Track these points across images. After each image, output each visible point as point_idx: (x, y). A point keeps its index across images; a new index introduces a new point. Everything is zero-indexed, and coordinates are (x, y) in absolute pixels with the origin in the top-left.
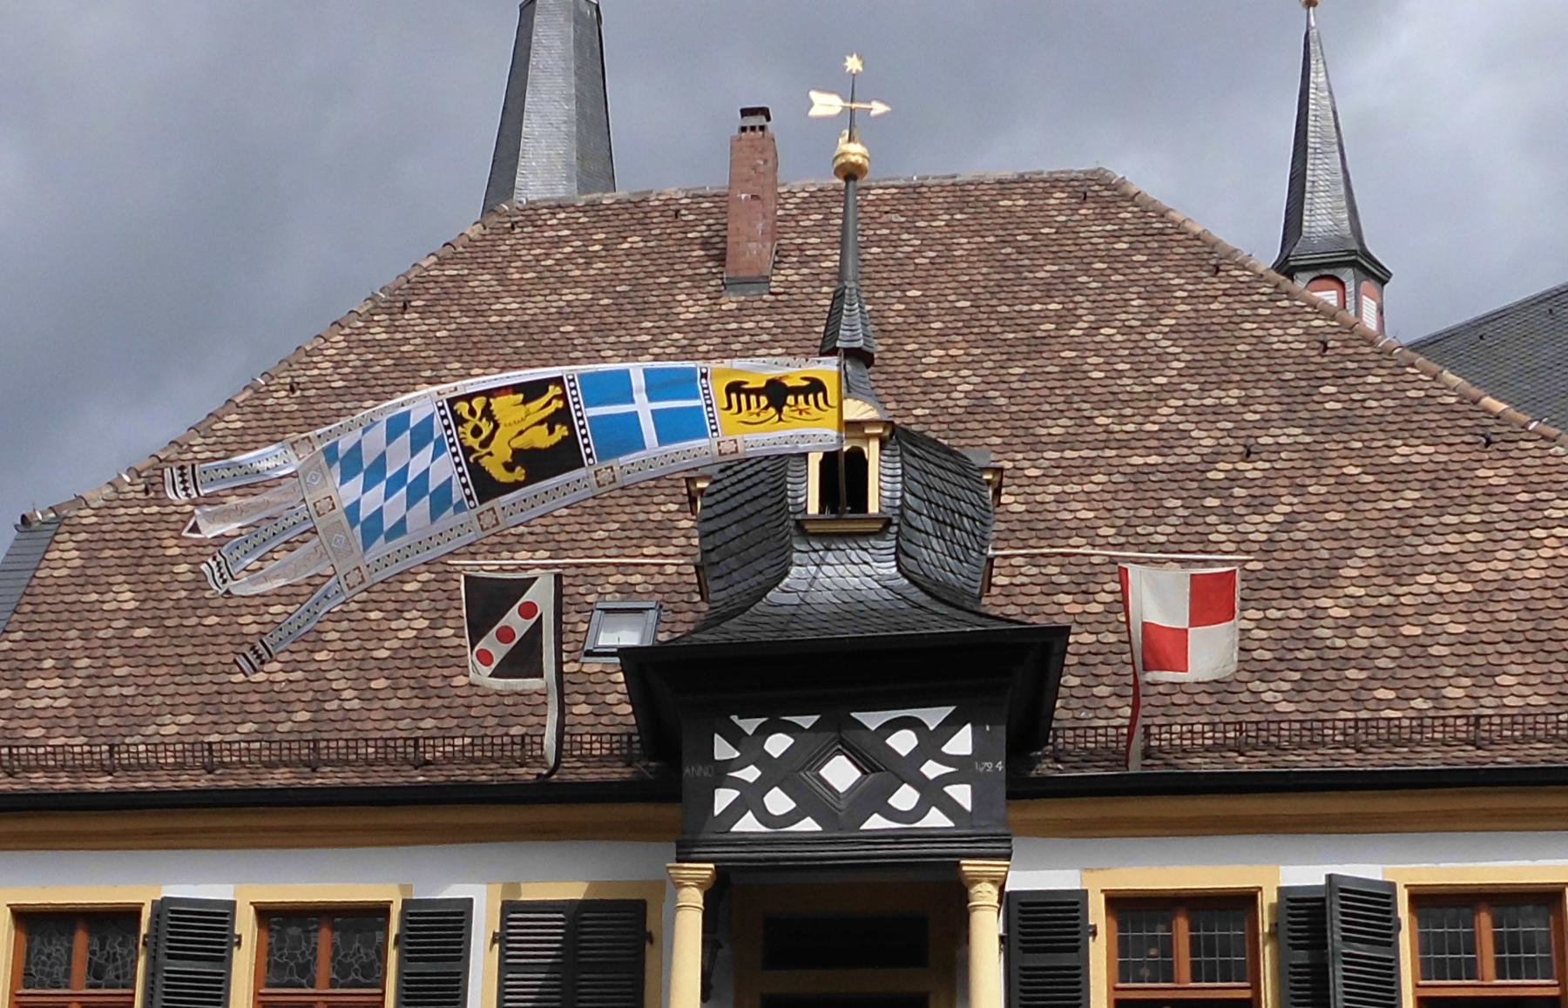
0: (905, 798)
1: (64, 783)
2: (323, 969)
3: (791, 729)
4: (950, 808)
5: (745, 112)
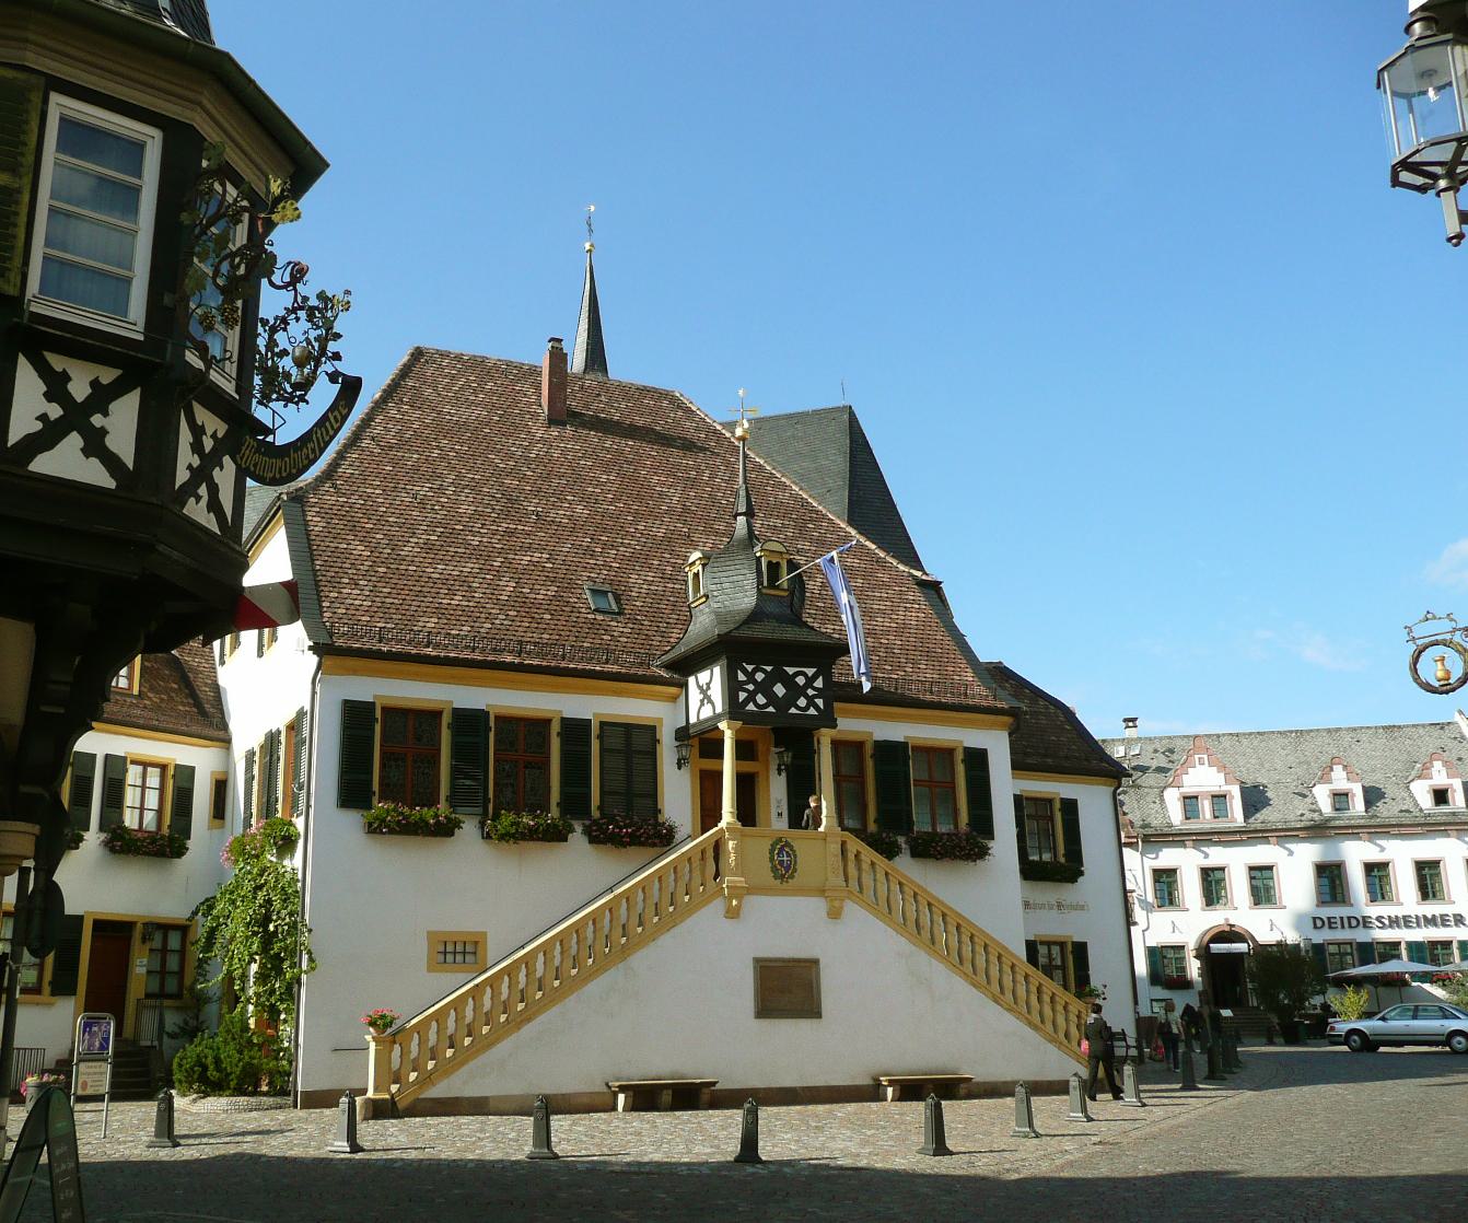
0: (802, 702)
3: (764, 671)
4: (817, 707)
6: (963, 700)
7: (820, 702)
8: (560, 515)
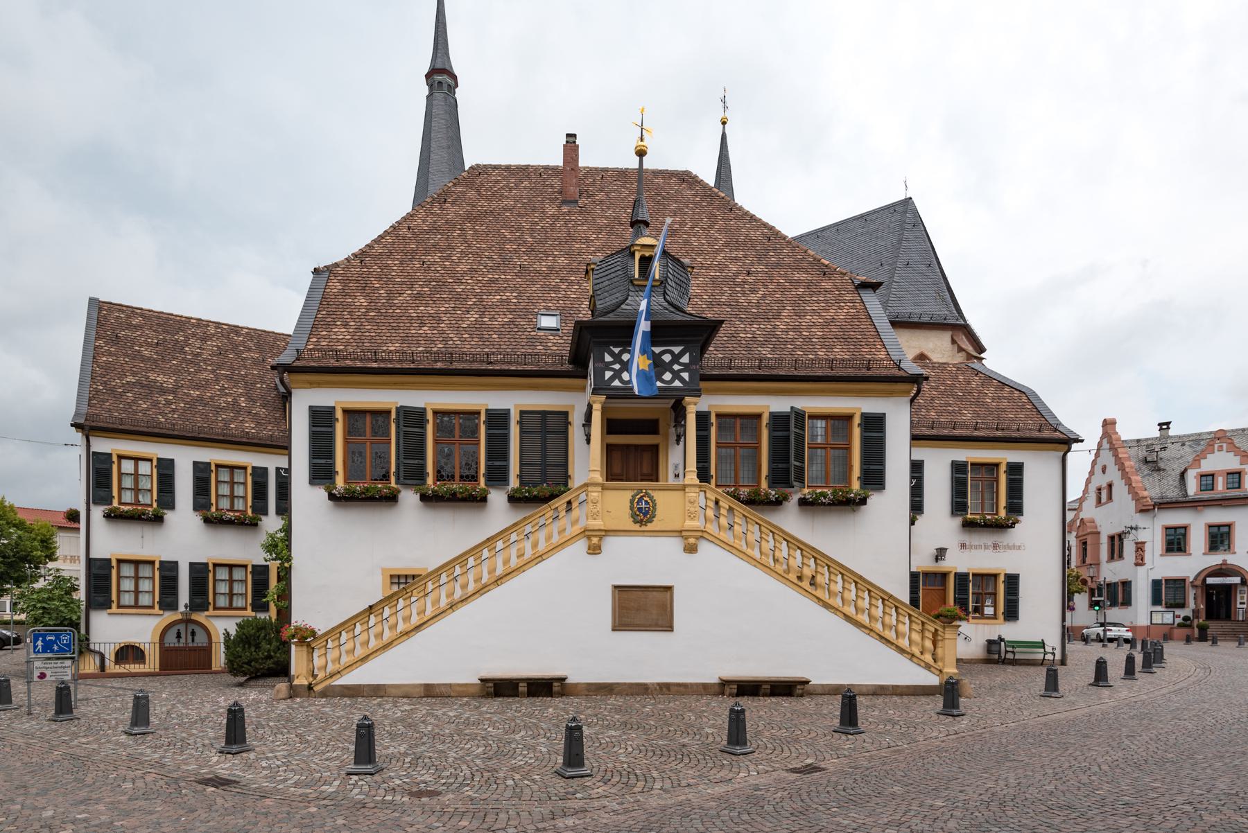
0: (667, 376)
4: (682, 380)
6: (864, 372)
7: (685, 375)
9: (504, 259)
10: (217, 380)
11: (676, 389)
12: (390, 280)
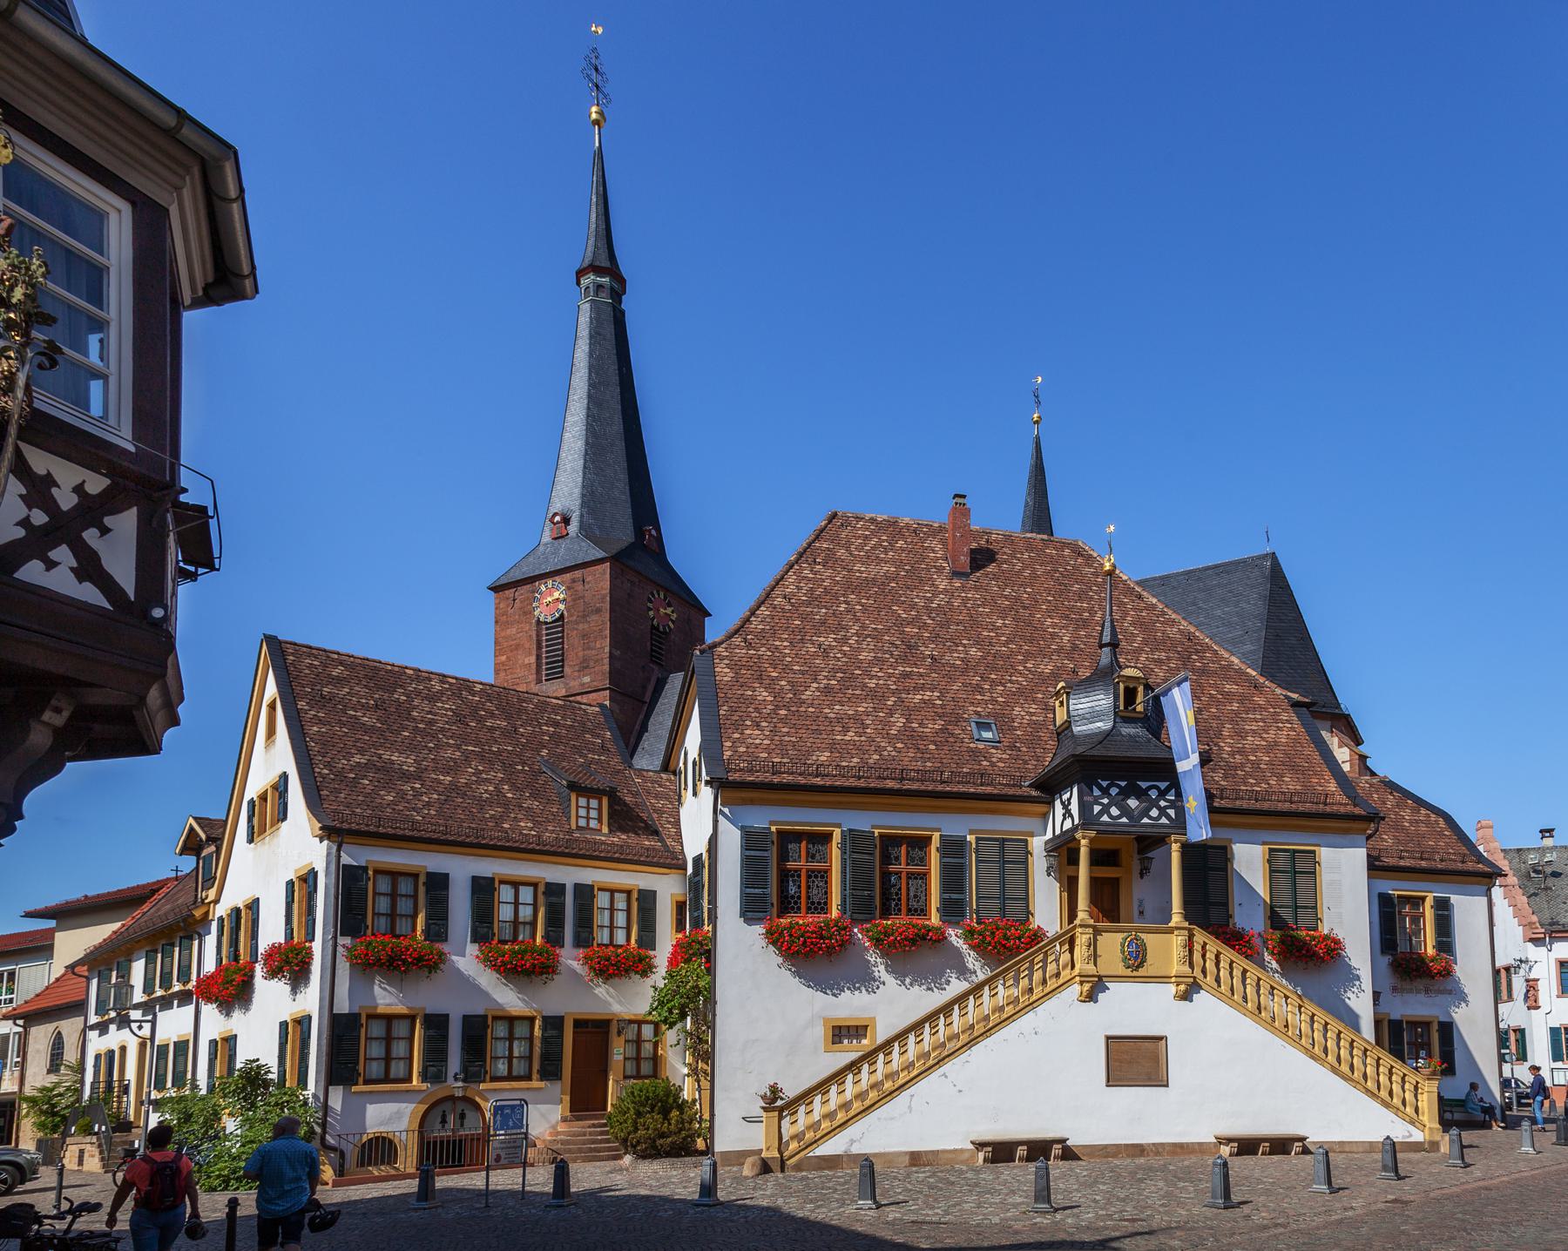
0: (1154, 813)
1: (801, 780)
2: (903, 859)
3: (1118, 786)
4: (1168, 817)
5: (956, 496)
8: (955, 658)
9: (909, 647)
10: (467, 758)
11: (1163, 826)
12: (787, 668)
